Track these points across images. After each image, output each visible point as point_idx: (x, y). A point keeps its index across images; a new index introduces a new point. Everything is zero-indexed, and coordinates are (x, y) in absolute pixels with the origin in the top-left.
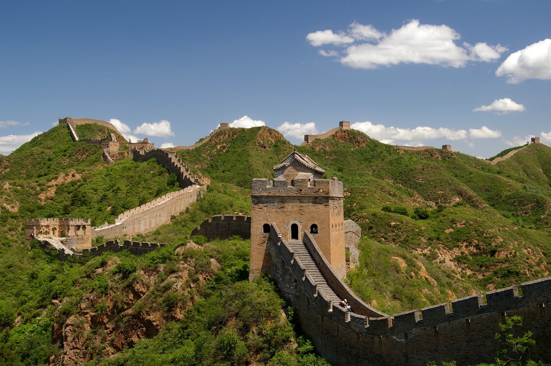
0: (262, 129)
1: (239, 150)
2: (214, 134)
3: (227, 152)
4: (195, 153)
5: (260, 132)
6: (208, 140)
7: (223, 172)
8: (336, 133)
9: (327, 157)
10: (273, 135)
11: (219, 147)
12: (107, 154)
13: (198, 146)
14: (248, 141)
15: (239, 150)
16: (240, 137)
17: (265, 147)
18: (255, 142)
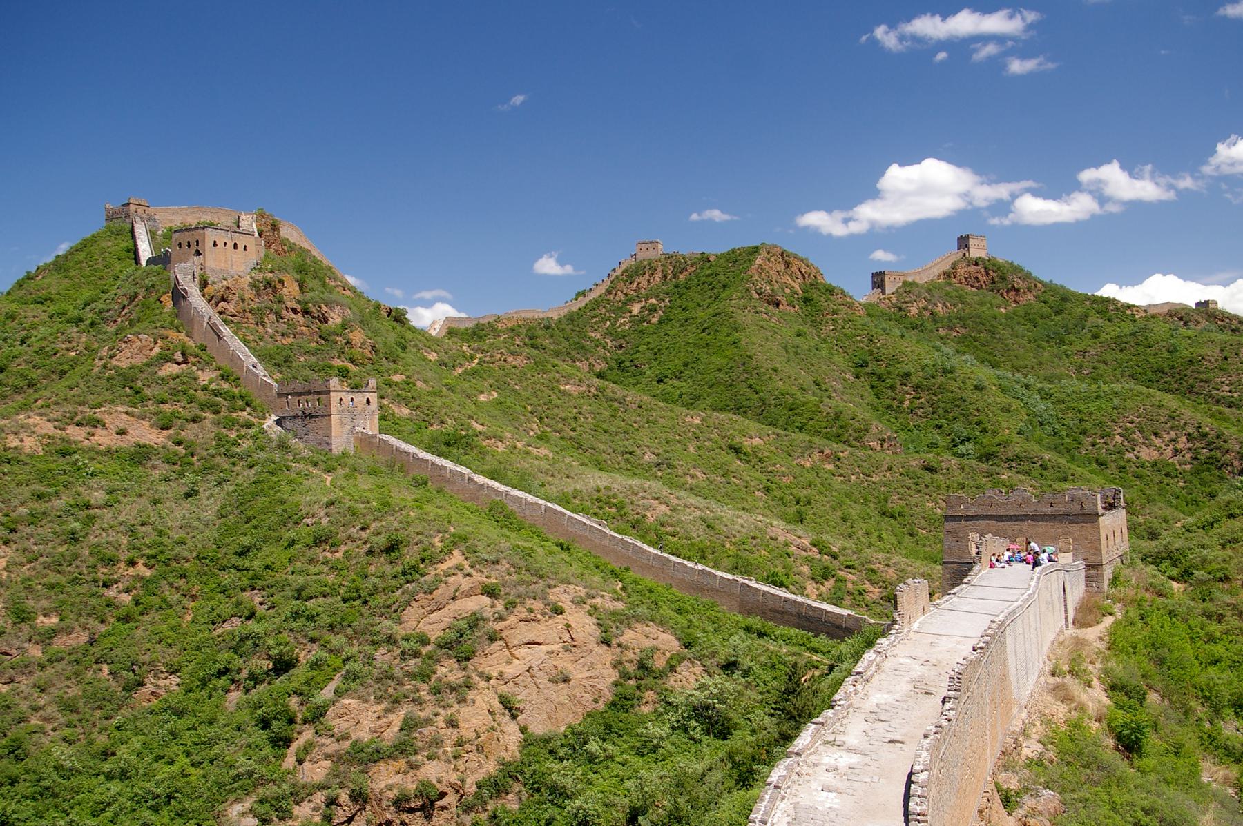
0: (764, 253)
1: (701, 314)
2: (619, 273)
3: (661, 322)
4: (568, 328)
5: (759, 261)
6: (601, 290)
7: (660, 381)
8: (954, 266)
9: (942, 332)
10: (794, 269)
11: (636, 309)
12: (193, 289)
13: (575, 309)
14: (725, 286)
15: (701, 314)
16: (698, 278)
17: (777, 304)
18: (747, 290)
